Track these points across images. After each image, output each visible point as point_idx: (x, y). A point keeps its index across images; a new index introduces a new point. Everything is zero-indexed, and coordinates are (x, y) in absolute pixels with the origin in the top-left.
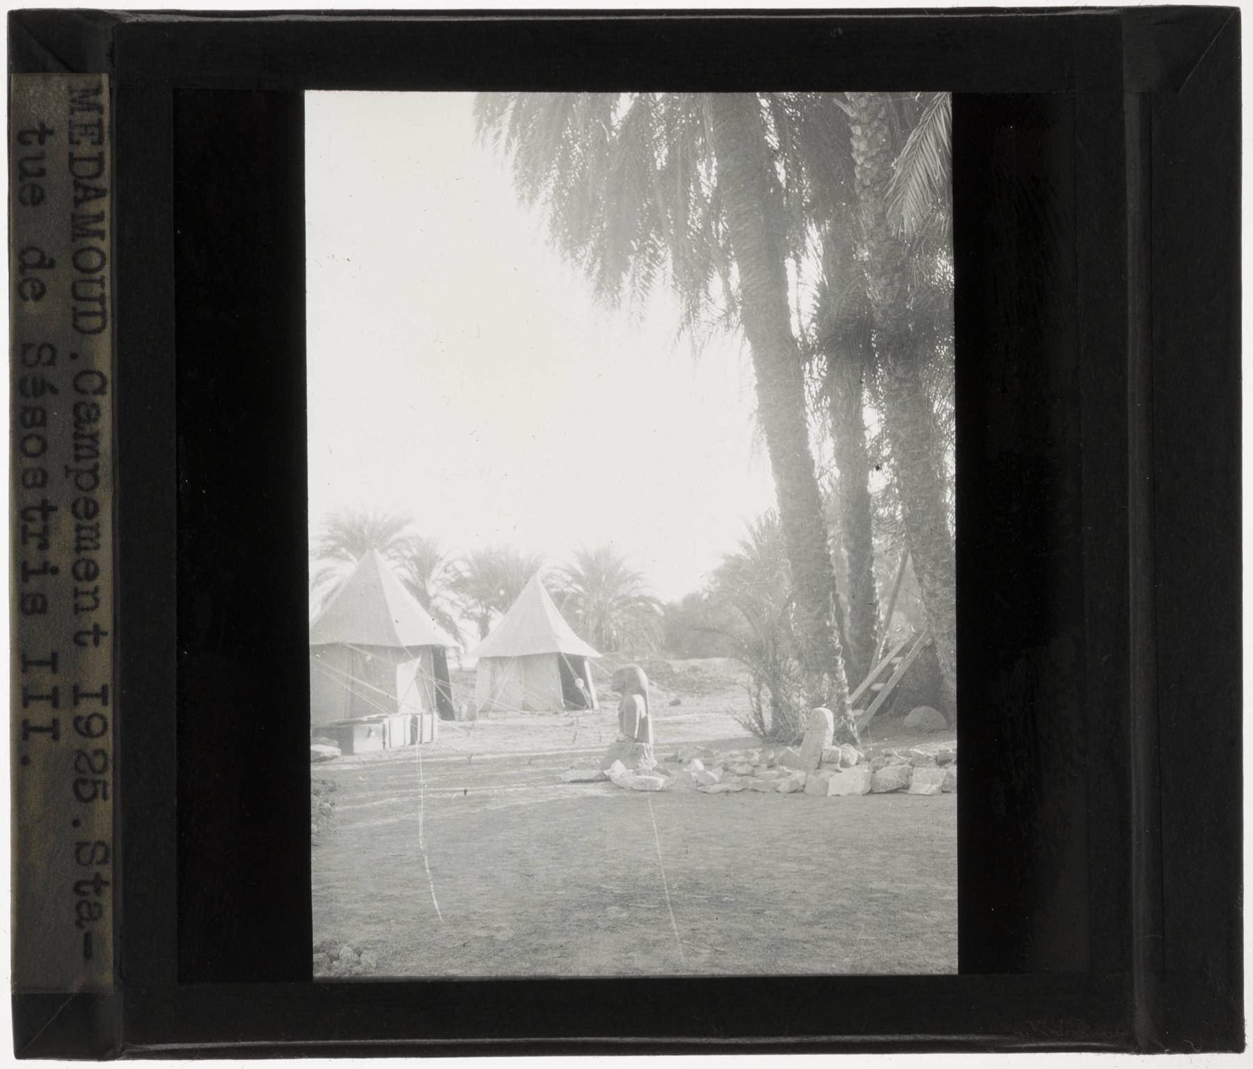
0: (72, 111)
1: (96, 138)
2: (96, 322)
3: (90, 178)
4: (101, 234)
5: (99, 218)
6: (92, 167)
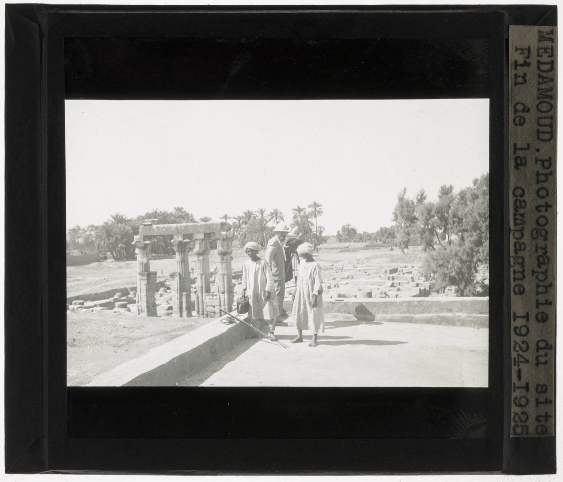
1: (550, 54)
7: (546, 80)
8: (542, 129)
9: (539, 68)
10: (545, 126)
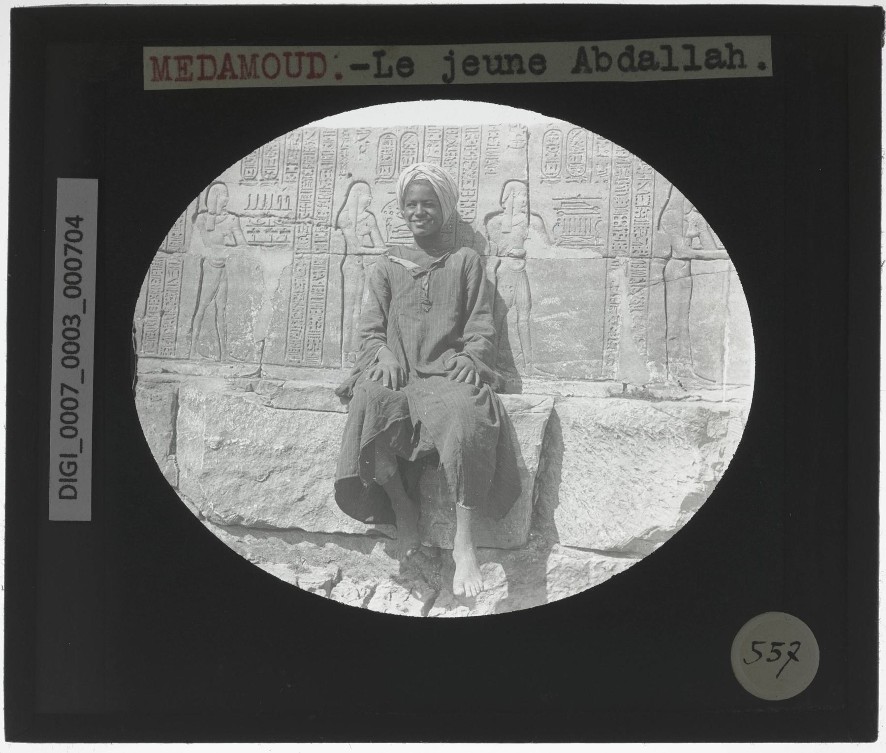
0: (168, 78)
2: (318, 61)
3: (215, 65)
4: (255, 56)
5: (242, 57)
6: (208, 64)
7: (228, 66)
8: (306, 70)
9: (210, 78)
10: (300, 68)
